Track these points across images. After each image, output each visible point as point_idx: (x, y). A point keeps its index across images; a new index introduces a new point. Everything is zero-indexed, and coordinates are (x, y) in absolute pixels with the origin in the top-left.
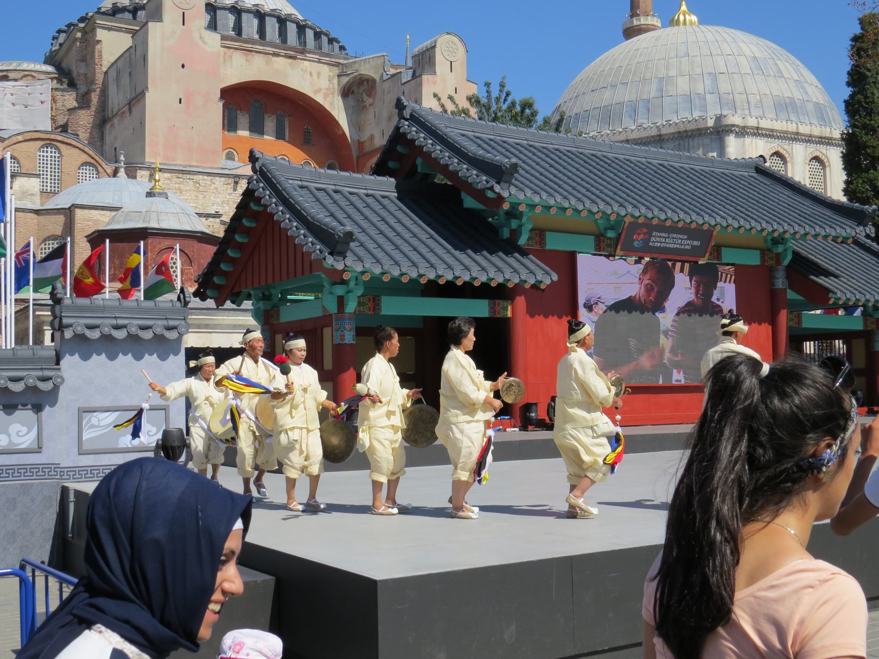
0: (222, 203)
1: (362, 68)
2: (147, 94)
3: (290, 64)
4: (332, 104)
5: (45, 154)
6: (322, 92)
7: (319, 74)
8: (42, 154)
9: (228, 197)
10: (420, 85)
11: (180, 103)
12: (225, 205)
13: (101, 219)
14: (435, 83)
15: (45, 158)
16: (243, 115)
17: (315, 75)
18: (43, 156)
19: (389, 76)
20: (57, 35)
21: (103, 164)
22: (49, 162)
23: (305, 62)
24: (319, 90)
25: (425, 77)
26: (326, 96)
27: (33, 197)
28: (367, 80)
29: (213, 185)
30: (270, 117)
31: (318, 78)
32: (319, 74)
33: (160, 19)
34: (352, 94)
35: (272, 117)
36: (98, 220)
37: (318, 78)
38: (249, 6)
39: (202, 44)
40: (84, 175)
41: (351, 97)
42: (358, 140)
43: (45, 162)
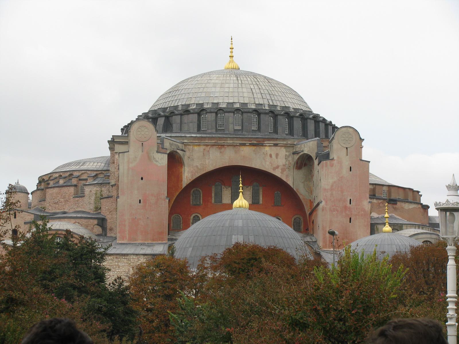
3: (254, 151)
4: (287, 176)
6: (280, 168)
7: (277, 155)
11: (140, 202)
14: (332, 165)
16: (227, 188)
17: (274, 156)
24: (278, 167)
26: (283, 170)
30: (248, 187)
31: (277, 158)
32: (277, 155)
34: (304, 166)
35: (249, 187)
37: (277, 158)
42: (310, 200)
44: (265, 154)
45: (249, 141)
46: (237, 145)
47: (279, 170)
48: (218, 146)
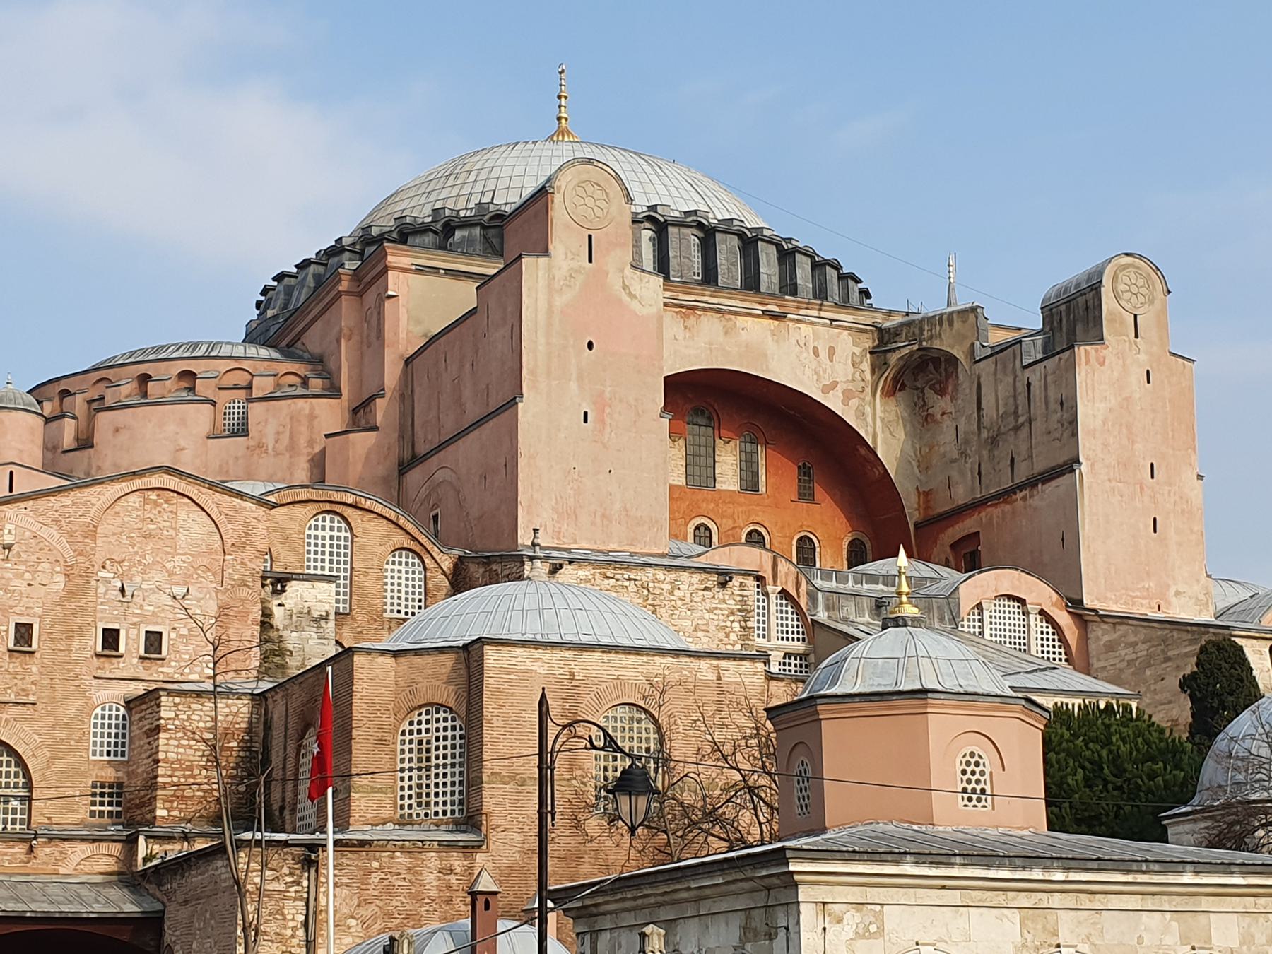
0: (695, 630)
1: (926, 334)
2: (520, 405)
4: (861, 414)
5: (320, 533)
6: (838, 388)
7: (832, 351)
8: (313, 532)
9: (706, 616)
10: (1071, 366)
11: (586, 421)
12: (700, 634)
13: (533, 668)
15: (320, 542)
17: (823, 354)
18: (316, 537)
19: (989, 352)
20: (275, 284)
21: (435, 551)
22: (327, 549)
23: (802, 326)
24: (834, 385)
25: (1081, 351)
26: (848, 396)
27: (323, 623)
28: (936, 361)
29: (677, 592)
30: (728, 442)
32: (832, 351)
33: (545, 251)
34: (900, 390)
35: (732, 443)
36: (527, 671)
38: (677, 214)
39: (626, 298)
40: (396, 574)
41: (898, 394)
43: (319, 549)
44: (802, 345)
45: (760, 303)
46: (730, 312)
47: (838, 392)
48: (678, 310)
